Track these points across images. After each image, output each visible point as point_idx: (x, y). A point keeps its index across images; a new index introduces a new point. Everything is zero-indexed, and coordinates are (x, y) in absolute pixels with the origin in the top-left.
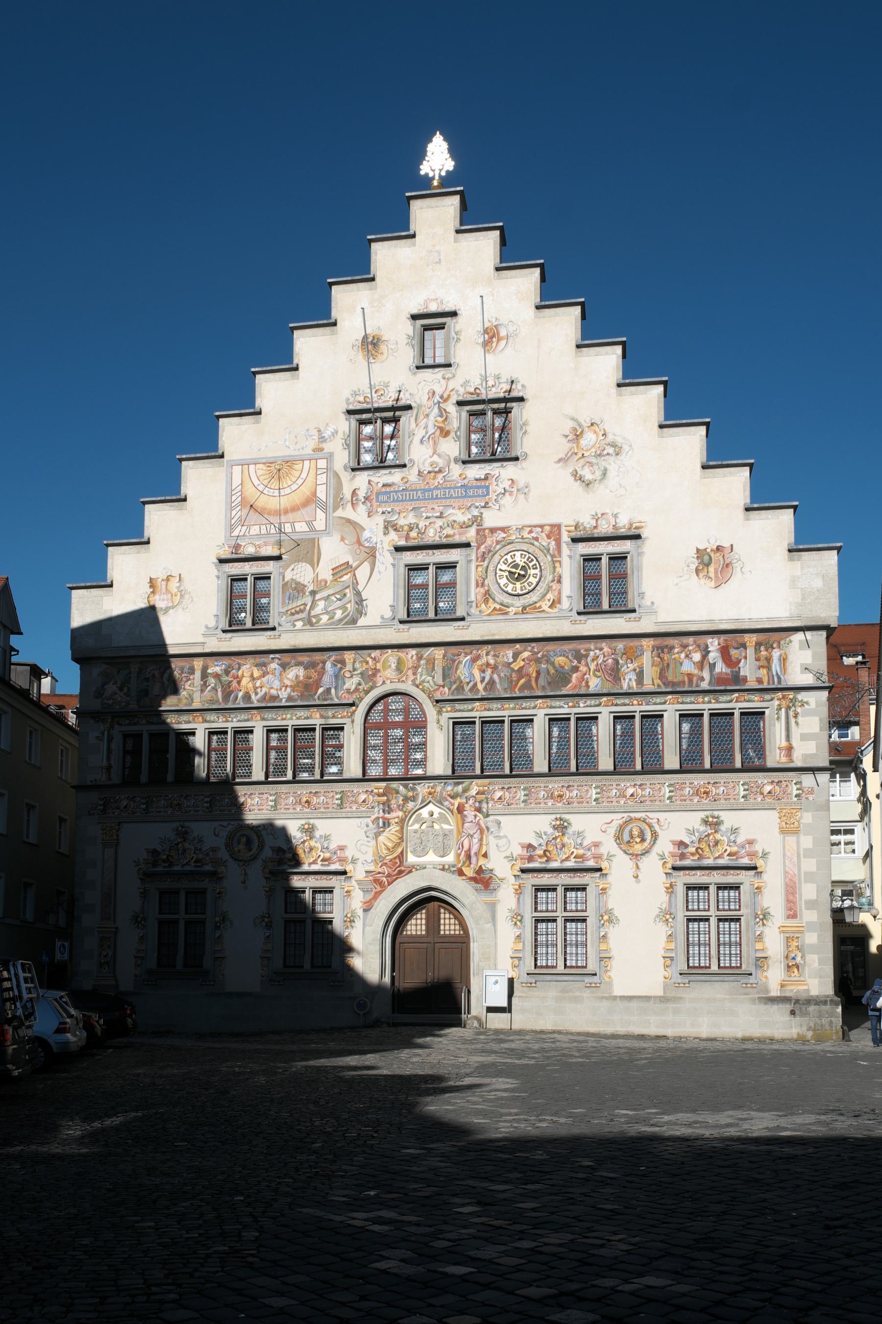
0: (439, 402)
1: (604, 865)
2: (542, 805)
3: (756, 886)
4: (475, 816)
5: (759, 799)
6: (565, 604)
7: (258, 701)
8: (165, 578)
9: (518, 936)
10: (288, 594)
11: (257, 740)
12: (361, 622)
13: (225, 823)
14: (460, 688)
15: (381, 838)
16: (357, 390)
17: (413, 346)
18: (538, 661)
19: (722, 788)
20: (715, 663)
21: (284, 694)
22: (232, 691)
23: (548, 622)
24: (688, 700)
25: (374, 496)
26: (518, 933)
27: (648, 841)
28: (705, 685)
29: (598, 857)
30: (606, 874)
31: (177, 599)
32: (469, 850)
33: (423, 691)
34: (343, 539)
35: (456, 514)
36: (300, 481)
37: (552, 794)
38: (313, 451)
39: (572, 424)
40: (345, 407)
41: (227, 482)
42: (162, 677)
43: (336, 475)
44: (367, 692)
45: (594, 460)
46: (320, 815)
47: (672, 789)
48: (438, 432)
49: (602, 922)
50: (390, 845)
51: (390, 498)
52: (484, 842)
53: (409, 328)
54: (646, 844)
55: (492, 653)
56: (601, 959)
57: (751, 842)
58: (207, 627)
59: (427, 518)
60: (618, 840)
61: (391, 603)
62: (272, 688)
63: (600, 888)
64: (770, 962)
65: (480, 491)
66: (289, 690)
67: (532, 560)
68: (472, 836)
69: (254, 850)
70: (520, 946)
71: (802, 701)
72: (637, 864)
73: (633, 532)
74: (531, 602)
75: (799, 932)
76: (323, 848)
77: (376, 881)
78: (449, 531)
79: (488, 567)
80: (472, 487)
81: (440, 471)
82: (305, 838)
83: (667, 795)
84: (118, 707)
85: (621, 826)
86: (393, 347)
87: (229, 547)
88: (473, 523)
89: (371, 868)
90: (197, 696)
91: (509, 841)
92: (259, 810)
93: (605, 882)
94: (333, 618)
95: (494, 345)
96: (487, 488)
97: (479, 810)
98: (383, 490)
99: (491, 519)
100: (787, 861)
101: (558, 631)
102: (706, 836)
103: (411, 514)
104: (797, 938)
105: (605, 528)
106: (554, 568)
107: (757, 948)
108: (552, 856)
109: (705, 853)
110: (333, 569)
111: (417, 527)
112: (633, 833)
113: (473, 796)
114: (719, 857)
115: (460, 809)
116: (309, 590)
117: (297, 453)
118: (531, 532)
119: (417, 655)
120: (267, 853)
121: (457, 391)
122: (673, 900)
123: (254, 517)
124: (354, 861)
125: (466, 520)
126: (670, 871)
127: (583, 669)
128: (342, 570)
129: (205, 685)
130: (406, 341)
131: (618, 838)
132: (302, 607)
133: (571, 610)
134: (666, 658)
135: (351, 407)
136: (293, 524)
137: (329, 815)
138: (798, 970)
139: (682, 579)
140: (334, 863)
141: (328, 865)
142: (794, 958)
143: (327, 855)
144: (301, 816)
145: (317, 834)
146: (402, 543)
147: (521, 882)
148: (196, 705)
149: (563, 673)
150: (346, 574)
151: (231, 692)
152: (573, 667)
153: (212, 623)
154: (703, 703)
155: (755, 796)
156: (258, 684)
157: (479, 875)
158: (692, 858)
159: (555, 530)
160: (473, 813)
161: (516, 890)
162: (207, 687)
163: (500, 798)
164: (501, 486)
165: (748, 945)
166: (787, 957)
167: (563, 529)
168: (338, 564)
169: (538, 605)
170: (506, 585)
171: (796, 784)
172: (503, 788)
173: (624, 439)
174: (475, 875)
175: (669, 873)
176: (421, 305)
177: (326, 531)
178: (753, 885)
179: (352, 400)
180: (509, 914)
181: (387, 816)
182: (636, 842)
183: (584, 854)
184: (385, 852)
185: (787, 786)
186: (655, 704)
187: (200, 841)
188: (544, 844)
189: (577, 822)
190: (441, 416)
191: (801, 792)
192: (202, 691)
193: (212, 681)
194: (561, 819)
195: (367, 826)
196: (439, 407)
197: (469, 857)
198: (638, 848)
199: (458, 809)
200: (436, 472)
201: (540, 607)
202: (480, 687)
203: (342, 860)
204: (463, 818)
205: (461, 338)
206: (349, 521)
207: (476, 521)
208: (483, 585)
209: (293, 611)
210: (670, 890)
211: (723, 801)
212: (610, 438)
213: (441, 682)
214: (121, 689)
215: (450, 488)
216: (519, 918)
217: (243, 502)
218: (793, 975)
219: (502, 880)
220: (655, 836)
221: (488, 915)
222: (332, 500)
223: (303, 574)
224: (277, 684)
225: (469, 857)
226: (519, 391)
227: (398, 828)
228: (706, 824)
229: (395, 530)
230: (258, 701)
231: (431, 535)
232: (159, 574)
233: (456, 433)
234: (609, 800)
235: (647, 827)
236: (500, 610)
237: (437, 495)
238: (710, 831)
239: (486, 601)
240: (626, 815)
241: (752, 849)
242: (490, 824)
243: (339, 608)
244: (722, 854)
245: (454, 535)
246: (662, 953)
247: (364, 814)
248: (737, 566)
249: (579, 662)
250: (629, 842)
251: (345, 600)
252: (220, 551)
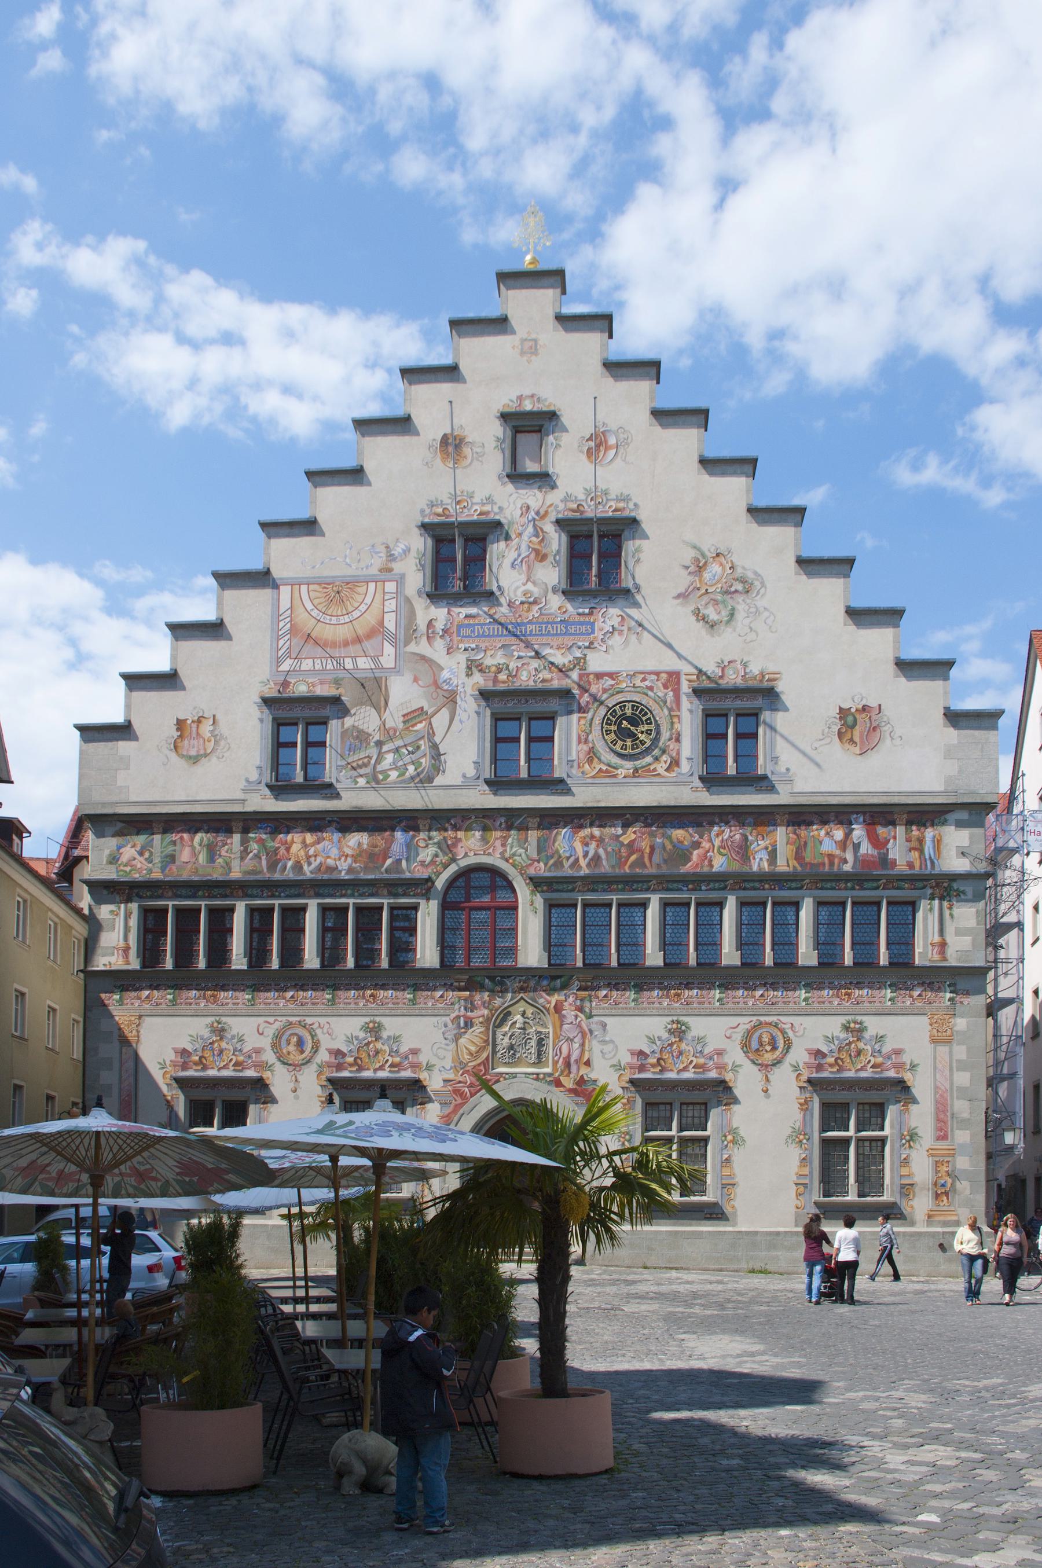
0: (534, 520)
2: (656, 1005)
4: (576, 1017)
5: (908, 1003)
6: (685, 767)
7: (311, 872)
8: (196, 718)
10: (348, 743)
11: (311, 920)
12: (438, 780)
13: (271, 1020)
14: (559, 864)
15: (462, 1041)
16: (434, 499)
17: (503, 452)
18: (652, 835)
20: (859, 843)
21: (344, 865)
22: (280, 860)
23: (664, 788)
24: (829, 885)
25: (454, 629)
27: (780, 1050)
28: (848, 868)
29: (721, 1067)
31: (210, 746)
32: (569, 1056)
33: (514, 865)
34: (416, 680)
35: (554, 655)
36: (363, 608)
38: (380, 571)
39: (692, 553)
40: (419, 519)
41: (273, 605)
42: (192, 840)
43: (408, 600)
44: (446, 866)
45: (719, 597)
46: (387, 1012)
48: (533, 556)
50: (473, 1049)
51: (473, 632)
53: (497, 429)
54: (778, 1053)
55: (597, 823)
56: (724, 1186)
57: (898, 1052)
58: (247, 781)
59: (519, 658)
61: (475, 759)
62: (329, 857)
64: (917, 1189)
65: (583, 628)
66: (349, 860)
67: (646, 714)
68: (572, 1040)
69: (306, 1053)
71: (957, 890)
73: (765, 684)
74: (644, 764)
75: (949, 1155)
76: (391, 1051)
77: (457, 1092)
78: (548, 676)
79: (592, 719)
80: (573, 623)
81: (535, 602)
82: (370, 1039)
84: (137, 875)
85: (749, 1031)
86: (479, 450)
87: (275, 684)
88: (575, 667)
89: (451, 1076)
90: (236, 864)
91: (617, 1047)
92: (313, 1004)
94: (403, 774)
95: (601, 454)
96: (593, 624)
97: (580, 1009)
98: (466, 622)
99: (596, 662)
100: (938, 1076)
101: (676, 799)
103: (500, 653)
104: (948, 1162)
105: (733, 678)
106: (672, 723)
109: (846, 1064)
110: (404, 716)
111: (507, 668)
114: (862, 1069)
115: (558, 1008)
116: (375, 739)
117: (360, 573)
118: (644, 680)
119: (506, 822)
120: (323, 1056)
121: (557, 507)
122: (808, 1117)
123: (309, 648)
124: (429, 1067)
125: (566, 661)
126: (805, 1085)
127: (706, 845)
128: (415, 717)
129: (245, 852)
130: (494, 444)
131: (745, 1046)
132: (366, 760)
133: (692, 775)
134: (803, 835)
135: (427, 520)
136: (354, 658)
137: (399, 1012)
139: (823, 742)
140: (405, 1070)
141: (398, 1072)
142: (943, 1185)
143: (397, 1060)
144: (364, 1012)
145: (385, 1035)
146: (490, 686)
148: (236, 874)
149: (682, 850)
150: (421, 722)
151: (278, 861)
152: (693, 842)
153: (254, 776)
154: (846, 889)
156: (312, 852)
159: (674, 677)
160: (573, 1013)
162: (248, 854)
164: (609, 623)
166: (935, 1184)
167: (683, 678)
168: (409, 710)
169: (652, 768)
170: (615, 744)
171: (949, 986)
172: (609, 984)
173: (756, 573)
174: (575, 1087)
176: (512, 401)
177: (396, 670)
179: (428, 511)
181: (469, 1014)
184: (467, 1057)
186: (790, 889)
187: (241, 1040)
189: (698, 1026)
190: (537, 536)
192: (242, 858)
193: (254, 847)
194: (678, 1022)
195: (446, 1026)
196: (535, 526)
197: (568, 1064)
198: (768, 1057)
199: (555, 1007)
200: (530, 603)
201: (655, 770)
202: (583, 863)
203: (415, 1066)
204: (562, 1018)
205: (562, 443)
206: (423, 658)
207: (578, 664)
208: (586, 741)
209: (354, 765)
211: (866, 1004)
212: (739, 571)
213: (535, 856)
214: (141, 854)
215: (548, 623)
216: (627, 1137)
217: (294, 630)
220: (788, 1045)
222: (402, 632)
223: (367, 719)
224: (334, 852)
225: (568, 1064)
226: (632, 510)
227: (482, 1029)
229: (480, 671)
230: (311, 872)
231: (524, 678)
232: (189, 717)
233: (555, 556)
235: (779, 1033)
236: (607, 771)
237: (531, 631)
238: (851, 1039)
239: (590, 761)
240: (754, 1019)
241: (899, 1060)
242: (593, 1027)
243: (413, 763)
245: (552, 679)
246: (794, 1178)
247: (442, 1012)
248: (886, 729)
249: (701, 837)
250: (757, 1050)
251: (419, 753)
252: (264, 689)
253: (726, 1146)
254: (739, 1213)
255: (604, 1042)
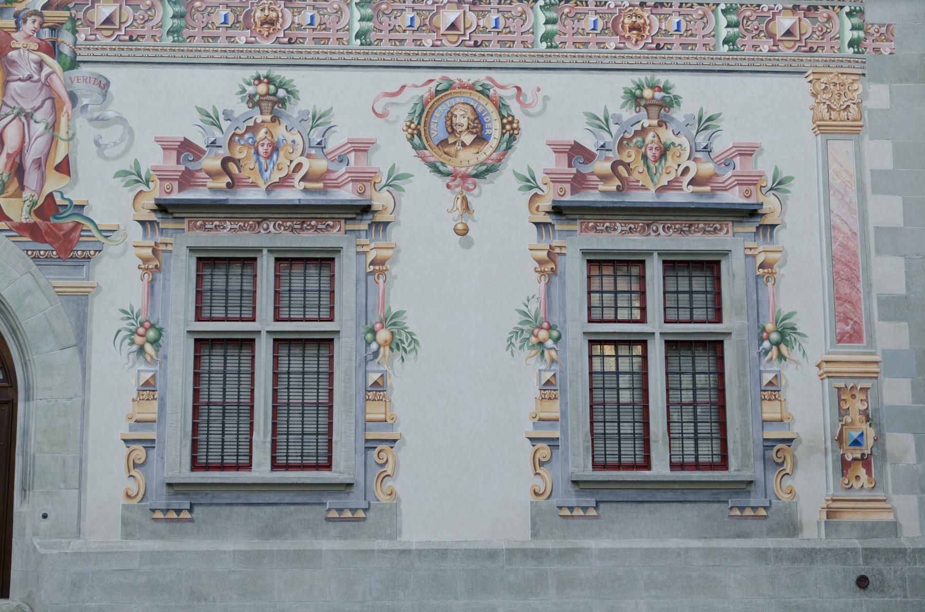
1: (380, 199)
2: (222, 43)
3: (760, 259)
4: (41, 64)
5: (765, 48)
9: (147, 383)
19: (675, 19)
26: (147, 376)
27: (493, 142)
29: (364, 179)
30: (386, 224)
32: (21, 152)
37: (247, 16)
47: (553, 15)
49: (374, 346)
52: (63, 132)
54: (488, 149)
57: (747, 152)
60: (416, 140)
63: (370, 257)
64: (800, 451)
68: (29, 116)
70: (150, 410)
72: (464, 199)
83: (542, 30)
91: (131, 132)
93: (381, 244)
97: (52, 49)
100: (833, 201)
102: (637, 133)
107: (766, 416)
108: (245, 173)
109: (635, 176)
112: (456, 121)
113: (35, 13)
114: (669, 187)
122: (556, 291)
126: (548, 219)
138: (869, 473)
142: (856, 443)
147: (160, 239)
155: (755, 41)
157: (46, 219)
158: (602, 187)
160: (34, 56)
161: (145, 260)
163: (109, 21)
165: (742, 407)
166: (840, 440)
171: (849, 14)
174: (33, 219)
175: (546, 224)
178: (754, 256)
180: (124, 324)
182: (464, 145)
183: (329, 171)
185: (829, 19)
188: (223, 139)
191: (862, 34)
194: (270, 81)
210: (548, 268)
211: (677, 50)
216: (152, 334)
218: (857, 485)
219: (108, 233)
221: (66, 327)
225: (18, 171)
228: (638, 105)
234: (394, 35)
235: (491, 108)
240: (437, 75)
242: (78, 87)
244: (676, 180)
250: (444, 143)
253: (376, 354)
254: (404, 507)
255: (100, 121)
